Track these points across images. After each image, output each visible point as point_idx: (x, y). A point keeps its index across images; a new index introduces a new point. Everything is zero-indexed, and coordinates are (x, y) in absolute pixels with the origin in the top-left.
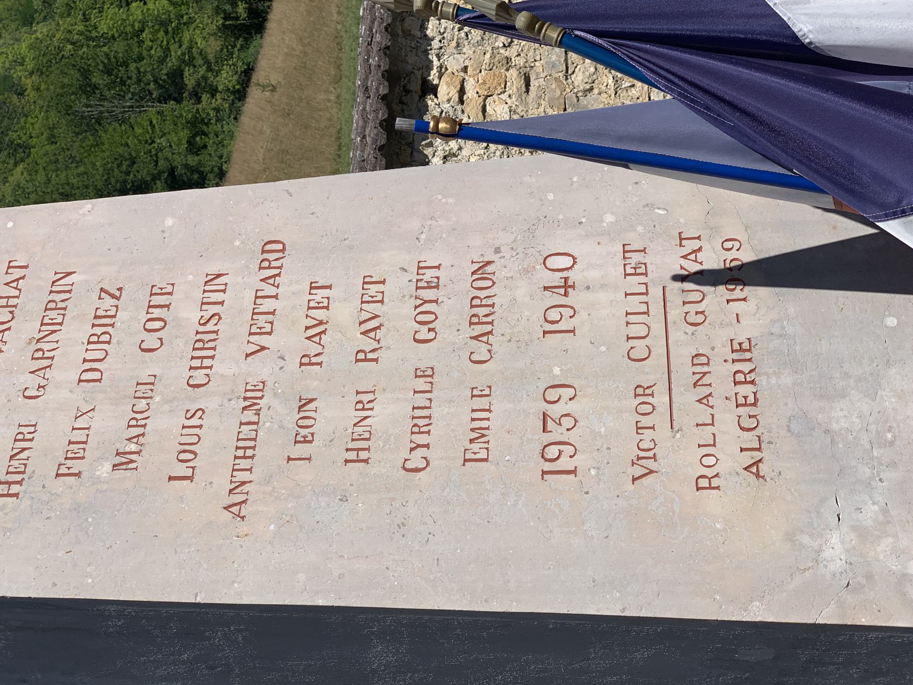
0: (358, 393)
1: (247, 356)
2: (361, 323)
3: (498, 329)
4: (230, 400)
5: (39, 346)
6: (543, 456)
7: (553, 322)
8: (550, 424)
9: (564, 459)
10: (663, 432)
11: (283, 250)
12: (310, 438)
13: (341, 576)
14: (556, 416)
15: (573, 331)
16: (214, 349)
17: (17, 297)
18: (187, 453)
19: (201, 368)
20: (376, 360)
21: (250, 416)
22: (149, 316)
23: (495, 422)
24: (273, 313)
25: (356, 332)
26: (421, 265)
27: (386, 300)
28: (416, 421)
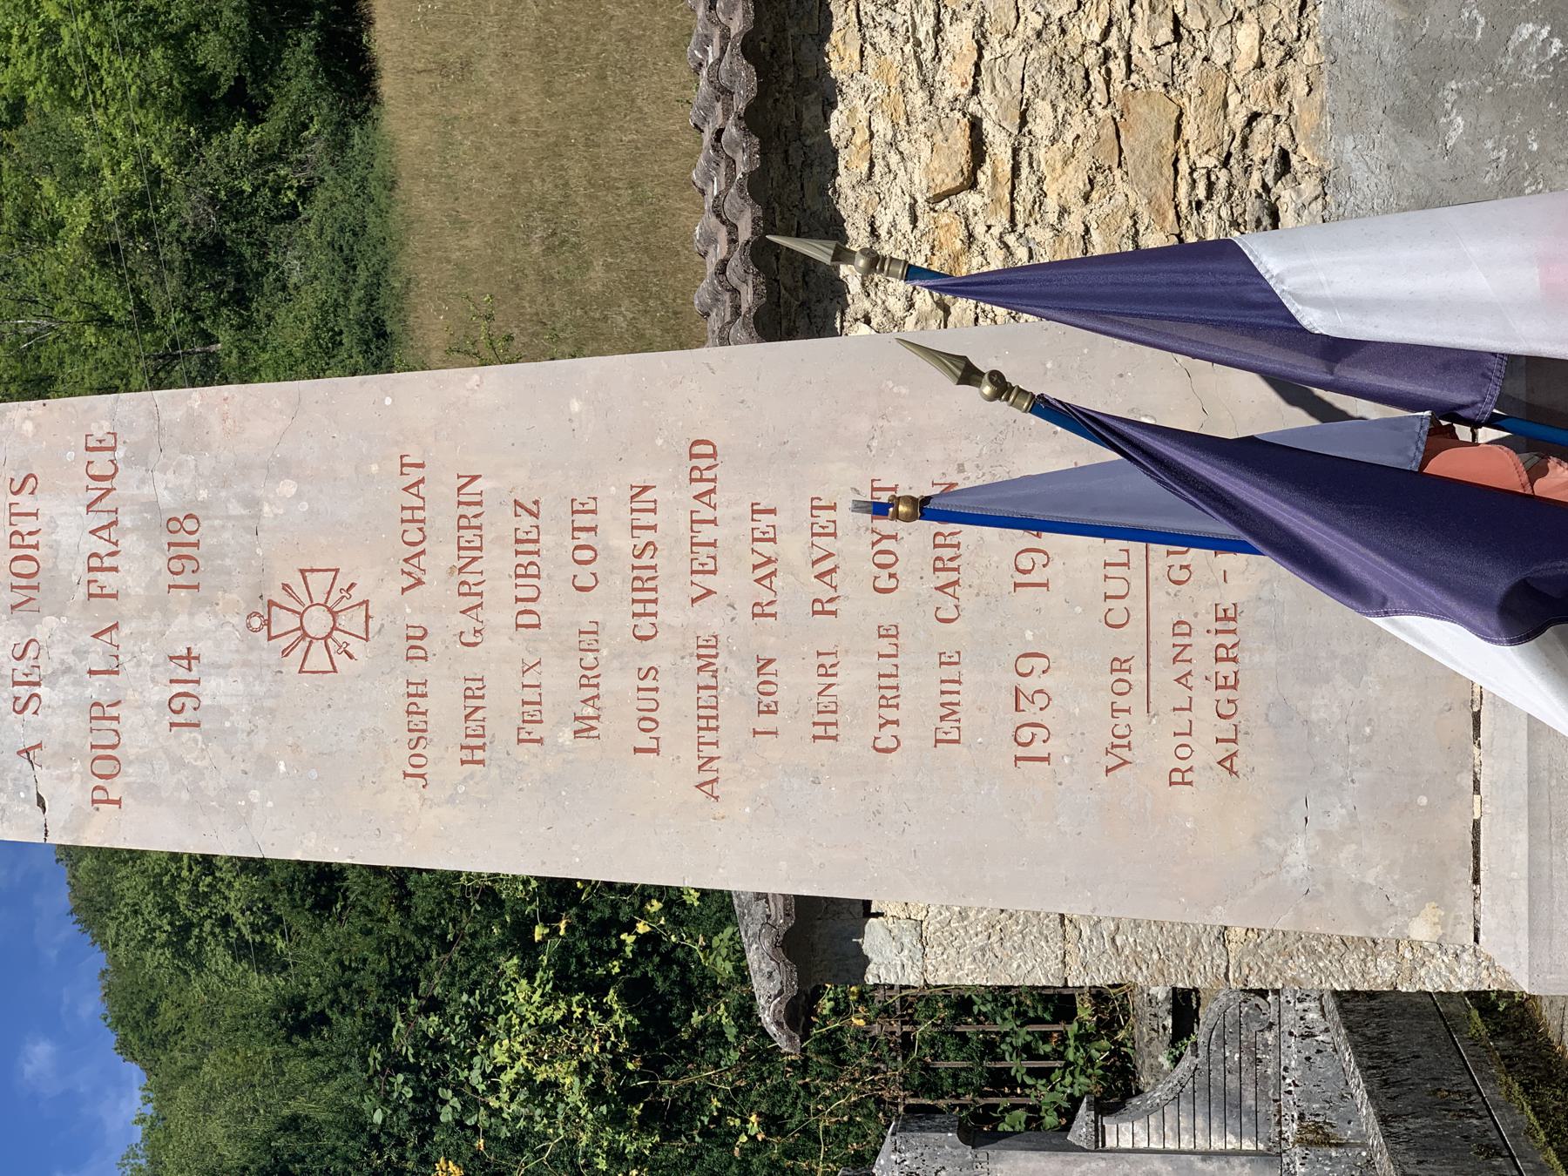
0: (819, 654)
1: (693, 601)
2: (814, 563)
3: (965, 577)
4: (683, 658)
5: (464, 577)
6: (1016, 740)
7: (1024, 572)
8: (1023, 702)
9: (1037, 744)
10: (1138, 717)
11: (714, 455)
12: (773, 708)
13: (822, 865)
14: (1029, 693)
15: (1046, 585)
16: (655, 590)
17: (422, 508)
18: (647, 720)
19: (645, 615)
20: (834, 613)
21: (705, 678)
22: (577, 542)
23: (966, 697)
24: (714, 544)
25: (809, 574)
26: (876, 485)
27: (839, 533)
28: (883, 692)
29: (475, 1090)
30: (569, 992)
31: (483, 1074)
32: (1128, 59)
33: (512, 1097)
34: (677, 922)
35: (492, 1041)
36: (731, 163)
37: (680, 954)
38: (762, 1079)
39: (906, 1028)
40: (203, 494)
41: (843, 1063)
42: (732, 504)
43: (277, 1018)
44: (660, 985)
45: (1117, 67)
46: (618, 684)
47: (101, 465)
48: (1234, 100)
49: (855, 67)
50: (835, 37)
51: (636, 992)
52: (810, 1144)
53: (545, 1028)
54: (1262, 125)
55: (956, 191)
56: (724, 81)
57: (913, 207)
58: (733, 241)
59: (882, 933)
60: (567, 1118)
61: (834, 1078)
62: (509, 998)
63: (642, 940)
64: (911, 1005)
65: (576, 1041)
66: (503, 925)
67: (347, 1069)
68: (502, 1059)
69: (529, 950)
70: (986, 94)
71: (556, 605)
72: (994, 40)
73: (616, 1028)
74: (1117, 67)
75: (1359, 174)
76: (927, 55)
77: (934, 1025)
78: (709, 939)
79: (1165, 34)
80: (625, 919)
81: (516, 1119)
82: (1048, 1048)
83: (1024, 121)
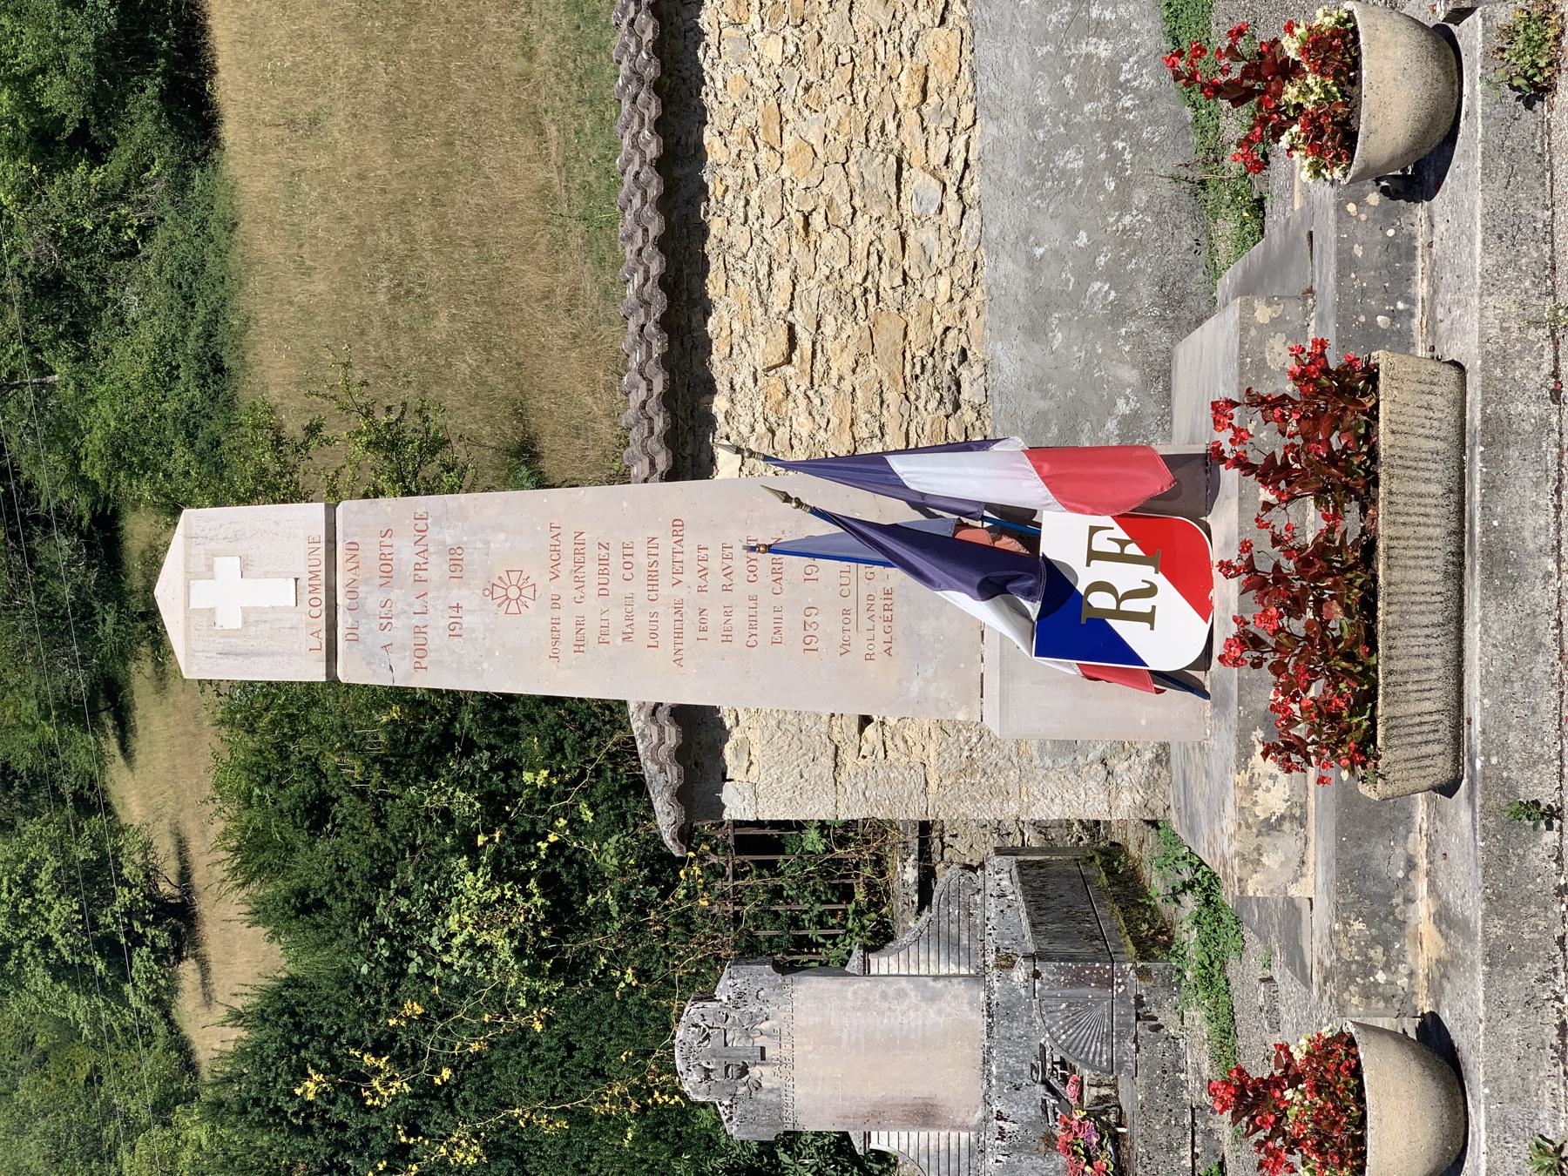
3: (784, 576)
10: (853, 632)
18: (653, 634)
21: (678, 617)
29: (433, 951)
30: (502, 881)
31: (440, 938)
32: (878, 294)
33: (461, 955)
34: (577, 834)
35: (447, 915)
36: (649, 345)
37: (579, 856)
38: (636, 944)
39: (736, 908)
40: (465, 539)
41: (693, 931)
42: (690, 545)
43: (289, 903)
44: (565, 878)
45: (871, 297)
46: (641, 619)
47: (421, 525)
48: (936, 318)
49: (723, 293)
50: (711, 275)
51: (549, 883)
52: (669, 989)
53: (485, 906)
54: (952, 334)
55: (780, 365)
56: (646, 297)
57: (755, 373)
58: (650, 390)
59: (733, 790)
60: (500, 969)
61: (687, 943)
62: (460, 886)
63: (552, 846)
64: (740, 892)
65: (507, 914)
66: (454, 836)
67: (341, 936)
68: (454, 927)
69: (473, 852)
70: (797, 310)
71: (616, 587)
72: (802, 280)
73: (536, 906)
74: (871, 297)
75: (1005, 363)
76: (764, 287)
77: (756, 905)
78: (599, 846)
79: (898, 281)
80: (540, 831)
81: (464, 969)
82: (834, 921)
83: (819, 327)
